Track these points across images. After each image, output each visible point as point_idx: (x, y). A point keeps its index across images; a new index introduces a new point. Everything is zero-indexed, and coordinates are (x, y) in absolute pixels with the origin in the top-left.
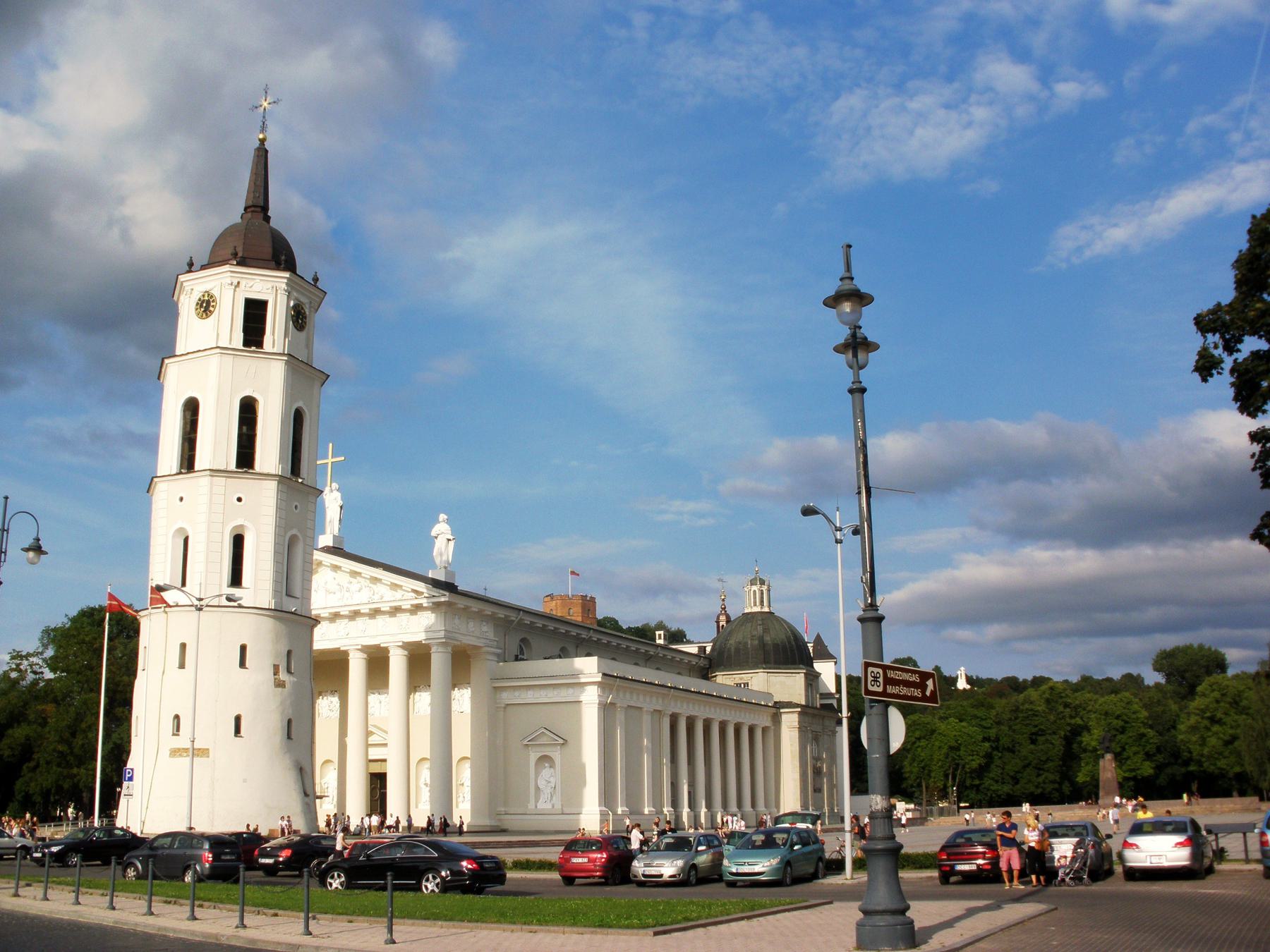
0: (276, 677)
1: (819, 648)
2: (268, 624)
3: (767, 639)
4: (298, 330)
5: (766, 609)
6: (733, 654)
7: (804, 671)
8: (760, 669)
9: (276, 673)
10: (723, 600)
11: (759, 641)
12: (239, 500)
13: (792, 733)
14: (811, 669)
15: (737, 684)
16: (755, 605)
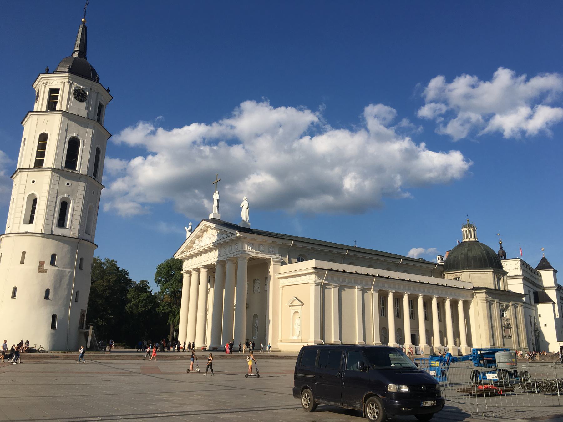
0: (42, 267)
1: (544, 263)
2: (40, 240)
3: (470, 254)
4: (79, 101)
5: (474, 240)
6: (452, 262)
7: (492, 270)
8: (465, 270)
9: (41, 264)
10: (501, 244)
11: (465, 256)
12: (33, 182)
13: (483, 304)
14: (502, 270)
15: (455, 278)
16: (467, 238)
